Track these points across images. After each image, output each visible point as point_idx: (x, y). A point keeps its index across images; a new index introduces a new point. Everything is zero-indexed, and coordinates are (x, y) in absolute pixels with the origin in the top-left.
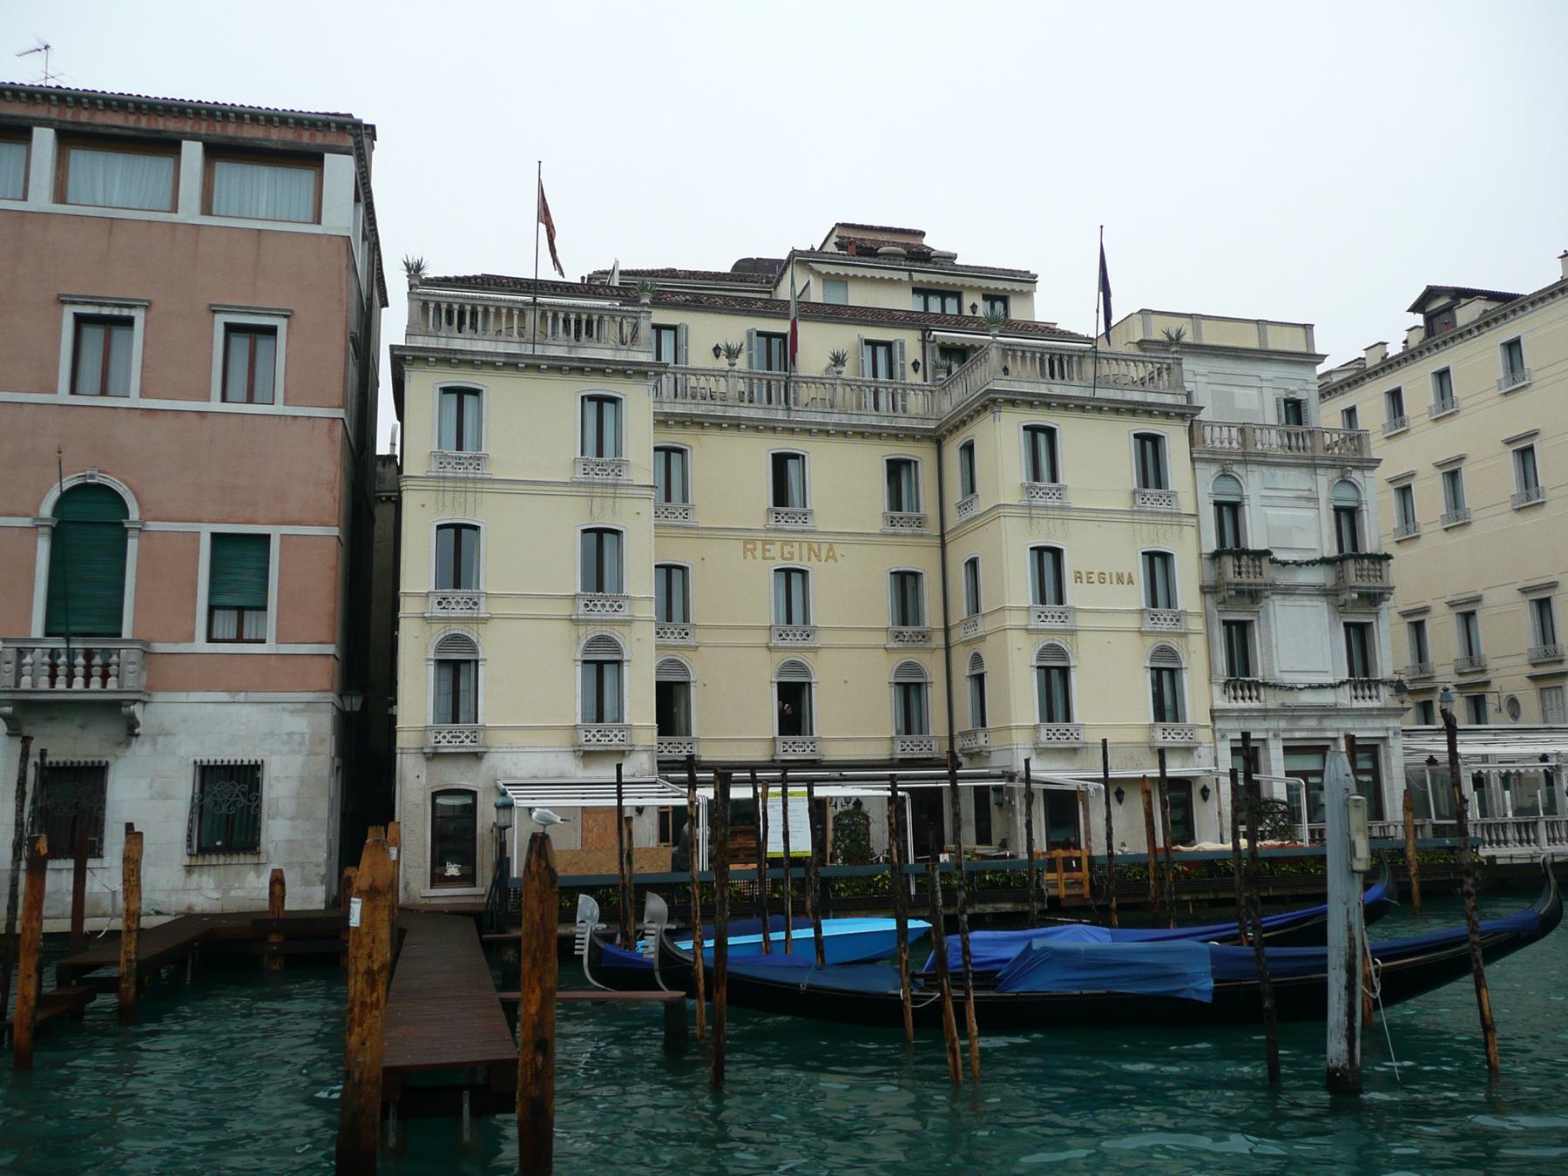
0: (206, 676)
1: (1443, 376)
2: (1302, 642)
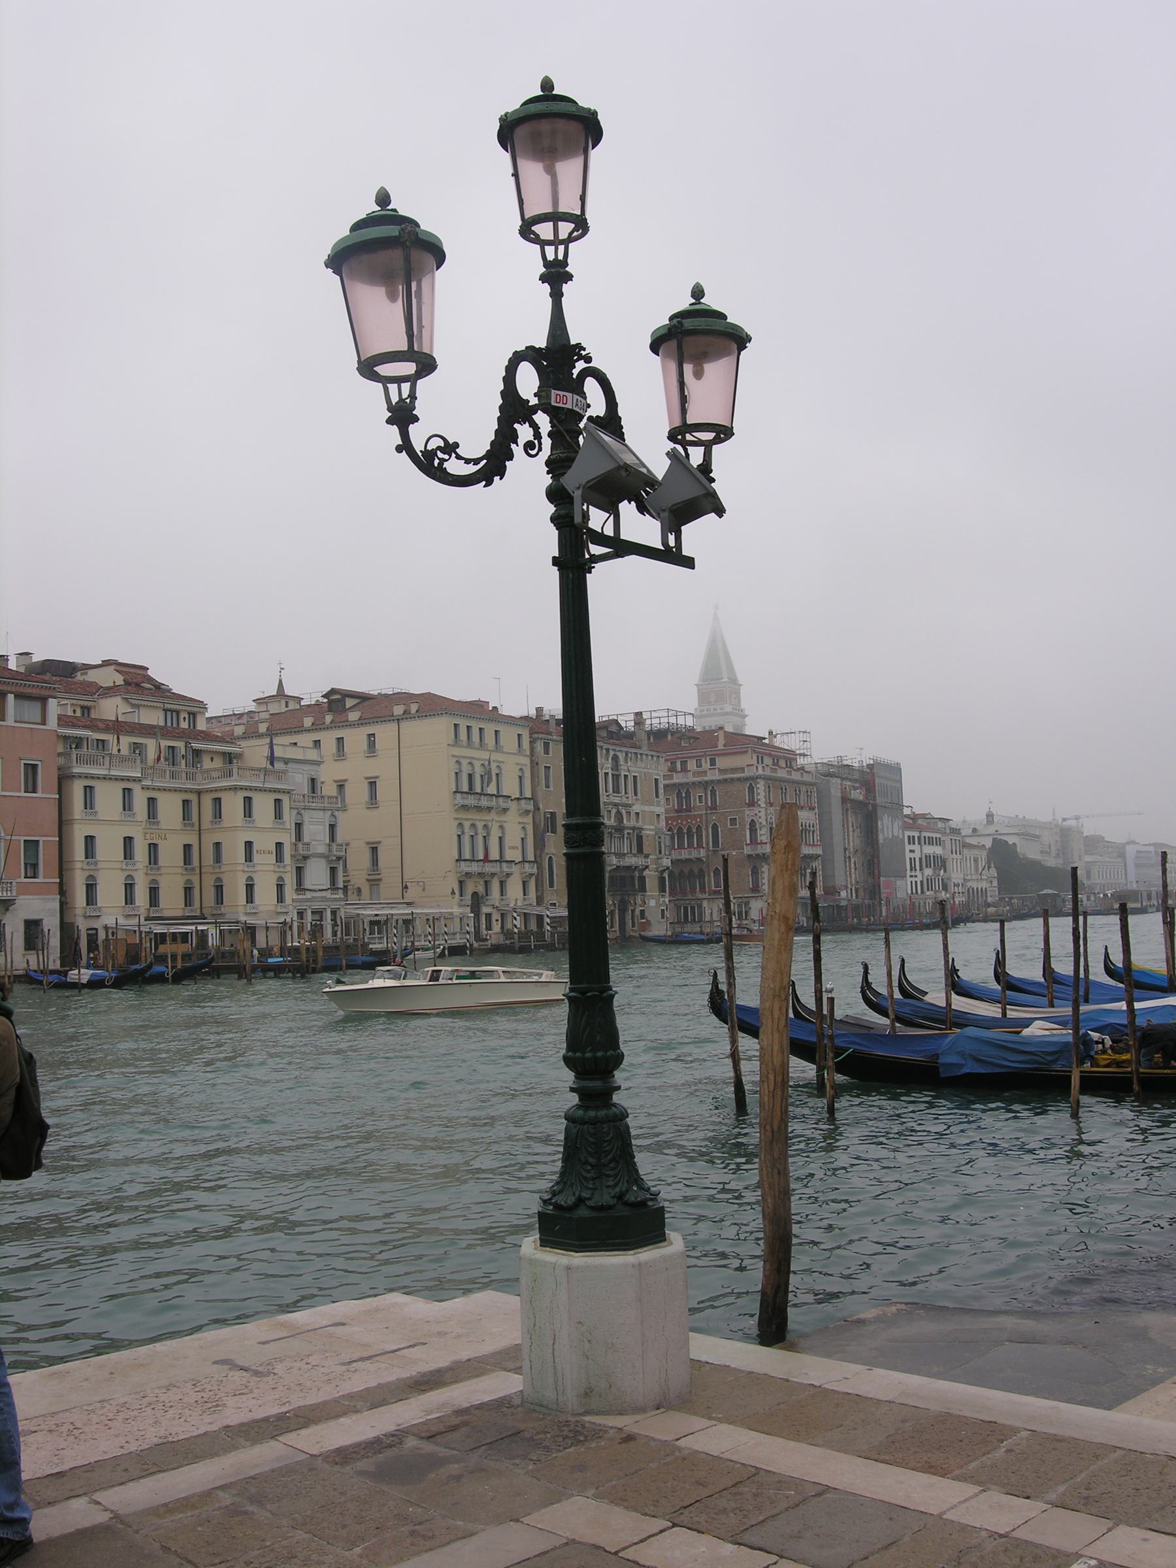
0: (24, 890)
1: (340, 740)
2: (317, 875)
